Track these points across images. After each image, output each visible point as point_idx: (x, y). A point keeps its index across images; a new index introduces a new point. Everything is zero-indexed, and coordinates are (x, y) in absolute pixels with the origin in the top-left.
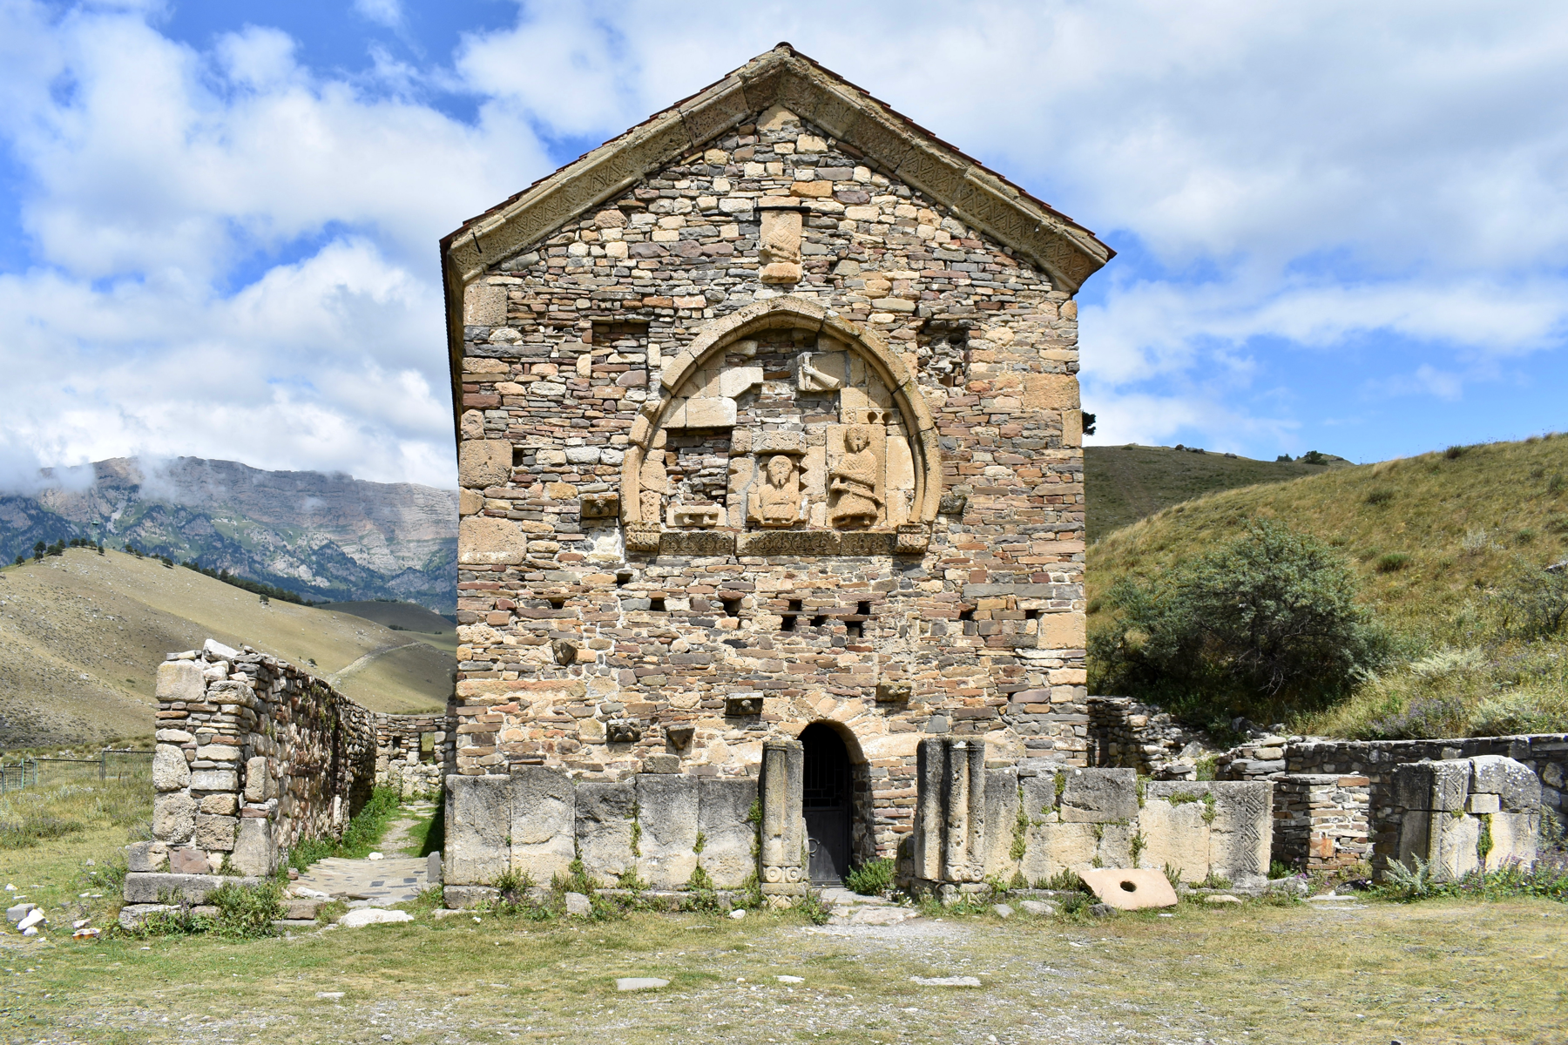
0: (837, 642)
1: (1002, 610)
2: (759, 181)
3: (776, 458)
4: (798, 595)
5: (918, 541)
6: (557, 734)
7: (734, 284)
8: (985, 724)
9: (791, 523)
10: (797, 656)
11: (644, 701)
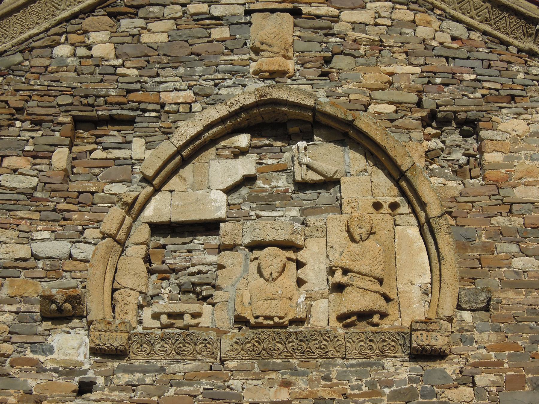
3: (267, 250)
7: (224, 79)
9: (286, 321)
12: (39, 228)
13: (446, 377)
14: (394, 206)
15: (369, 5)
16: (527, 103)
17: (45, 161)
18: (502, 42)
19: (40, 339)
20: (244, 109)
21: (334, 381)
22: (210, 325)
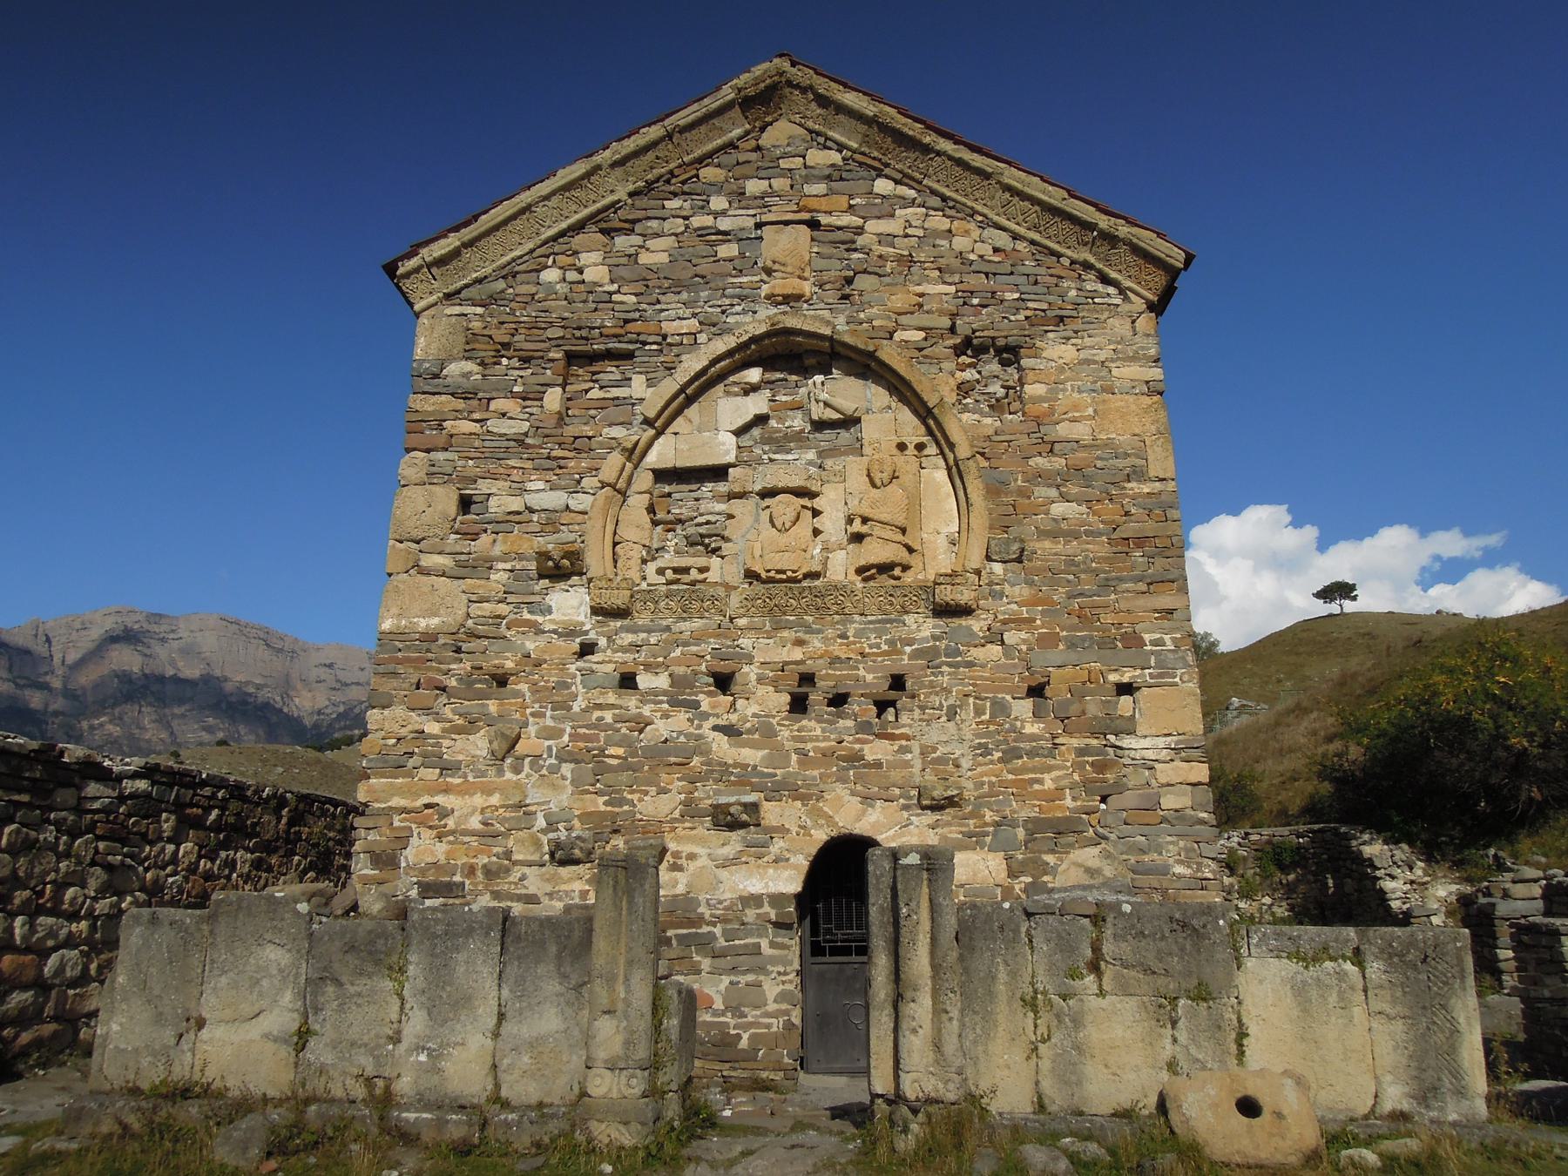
0: (864, 727)
1: (1084, 683)
2: (763, 198)
4: (810, 666)
5: (964, 596)
6: (482, 852)
8: (1071, 839)
9: (799, 575)
10: (809, 746)
11: (603, 808)
12: (533, 478)
13: (972, 634)
14: (920, 447)
15: (898, 212)
16: (1078, 325)
17: (536, 403)
18: (1053, 253)
19: (537, 598)
20: (754, 339)
21: (851, 639)
22: (718, 580)
